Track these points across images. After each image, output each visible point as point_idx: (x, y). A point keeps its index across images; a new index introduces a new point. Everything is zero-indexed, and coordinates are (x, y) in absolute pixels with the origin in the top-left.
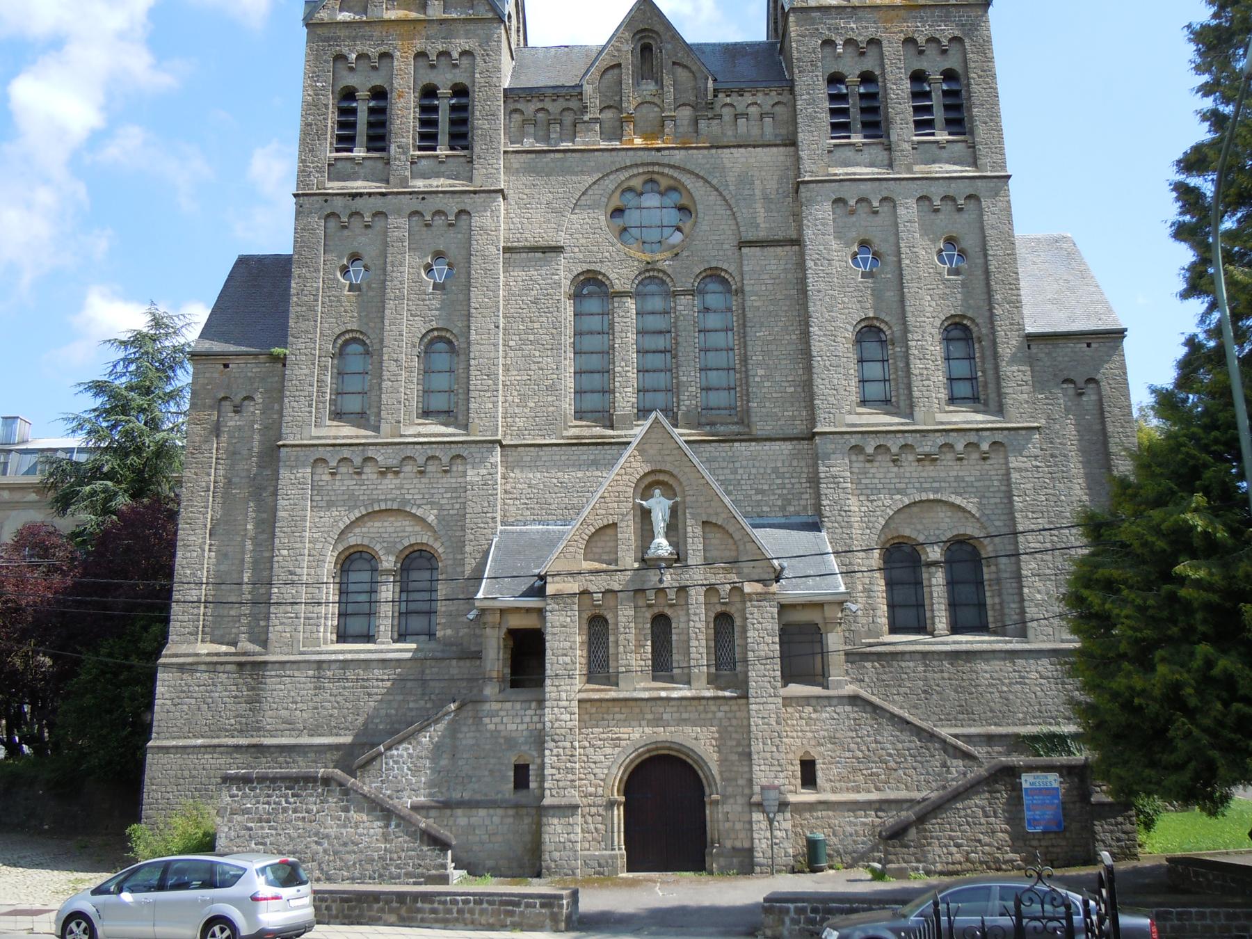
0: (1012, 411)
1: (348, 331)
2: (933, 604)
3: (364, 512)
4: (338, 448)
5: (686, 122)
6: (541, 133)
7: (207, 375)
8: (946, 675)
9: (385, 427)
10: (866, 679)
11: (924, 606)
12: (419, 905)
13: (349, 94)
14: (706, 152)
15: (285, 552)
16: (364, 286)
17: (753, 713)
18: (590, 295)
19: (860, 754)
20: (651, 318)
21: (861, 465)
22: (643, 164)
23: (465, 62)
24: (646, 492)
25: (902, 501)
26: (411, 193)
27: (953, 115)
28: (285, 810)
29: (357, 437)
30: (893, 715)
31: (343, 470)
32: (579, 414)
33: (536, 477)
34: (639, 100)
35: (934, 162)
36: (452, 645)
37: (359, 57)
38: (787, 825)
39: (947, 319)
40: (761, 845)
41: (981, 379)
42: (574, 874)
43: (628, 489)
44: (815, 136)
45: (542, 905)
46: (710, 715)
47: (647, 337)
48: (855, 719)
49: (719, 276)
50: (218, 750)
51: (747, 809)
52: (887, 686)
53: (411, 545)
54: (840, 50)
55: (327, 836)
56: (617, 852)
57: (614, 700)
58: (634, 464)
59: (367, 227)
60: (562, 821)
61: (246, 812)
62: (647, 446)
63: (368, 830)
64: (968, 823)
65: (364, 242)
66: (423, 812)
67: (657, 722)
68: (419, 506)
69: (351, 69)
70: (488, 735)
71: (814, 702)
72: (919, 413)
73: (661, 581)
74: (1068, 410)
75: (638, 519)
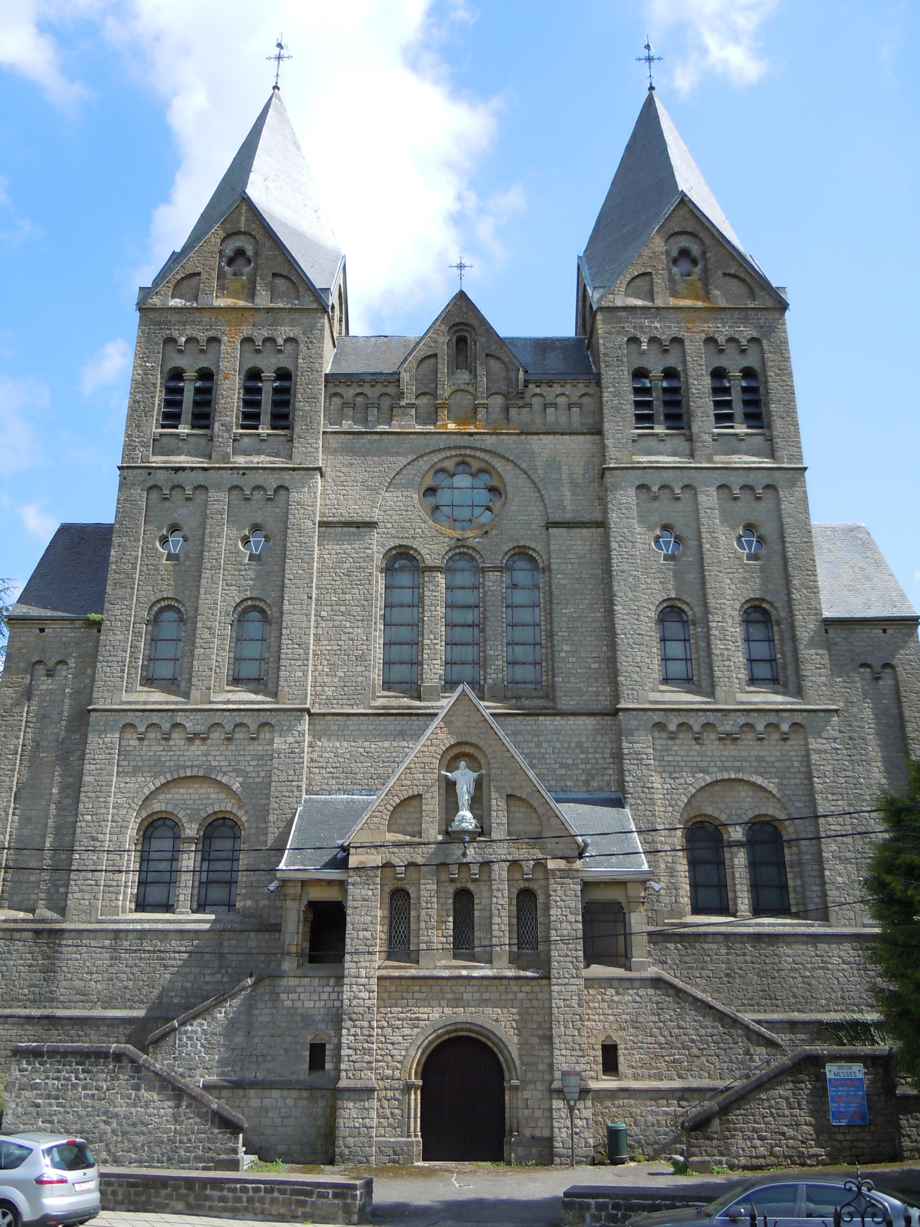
0: (811, 693)
1: (163, 599)
2: (735, 885)
3: (170, 779)
4: (147, 713)
5: (497, 410)
6: (359, 416)
7: (23, 639)
8: (748, 958)
9: (195, 694)
10: (669, 961)
11: (726, 886)
12: (208, 1192)
13: (177, 375)
14: (516, 438)
15: (89, 818)
16: (182, 555)
17: (555, 995)
18: (402, 569)
19: (663, 1040)
20: (460, 592)
21: (664, 742)
22: (455, 448)
23: (289, 348)
24: (451, 762)
25: (704, 780)
26: (232, 469)
27: (751, 410)
28: (74, 1086)
29: (167, 703)
30: (696, 1000)
31: (151, 735)
32: (387, 685)
33: (342, 746)
34: (454, 388)
35: (733, 453)
36: (251, 916)
37: (189, 340)
38: (588, 1113)
39: (747, 602)
40: (561, 1135)
41: (780, 661)
42: (368, 1161)
43: (434, 760)
44: (620, 425)
45: (336, 1196)
46: (511, 996)
47: (456, 611)
48: (657, 1003)
49: (527, 554)
50: (10, 1020)
51: (547, 1096)
52: (690, 968)
53: (215, 813)
54: (644, 347)
55: (116, 1115)
56: (413, 1139)
57: (414, 978)
58: (441, 736)
59: (188, 499)
60: (357, 1105)
61: (35, 1087)
62: (453, 718)
63: (158, 1109)
64: (772, 1114)
65: (183, 513)
66: (215, 1092)
67: (457, 1002)
68: (225, 773)
69: (180, 351)
70: (285, 1012)
71: (616, 984)
72: (720, 692)
73: (464, 855)
74: (865, 695)
75: (443, 791)
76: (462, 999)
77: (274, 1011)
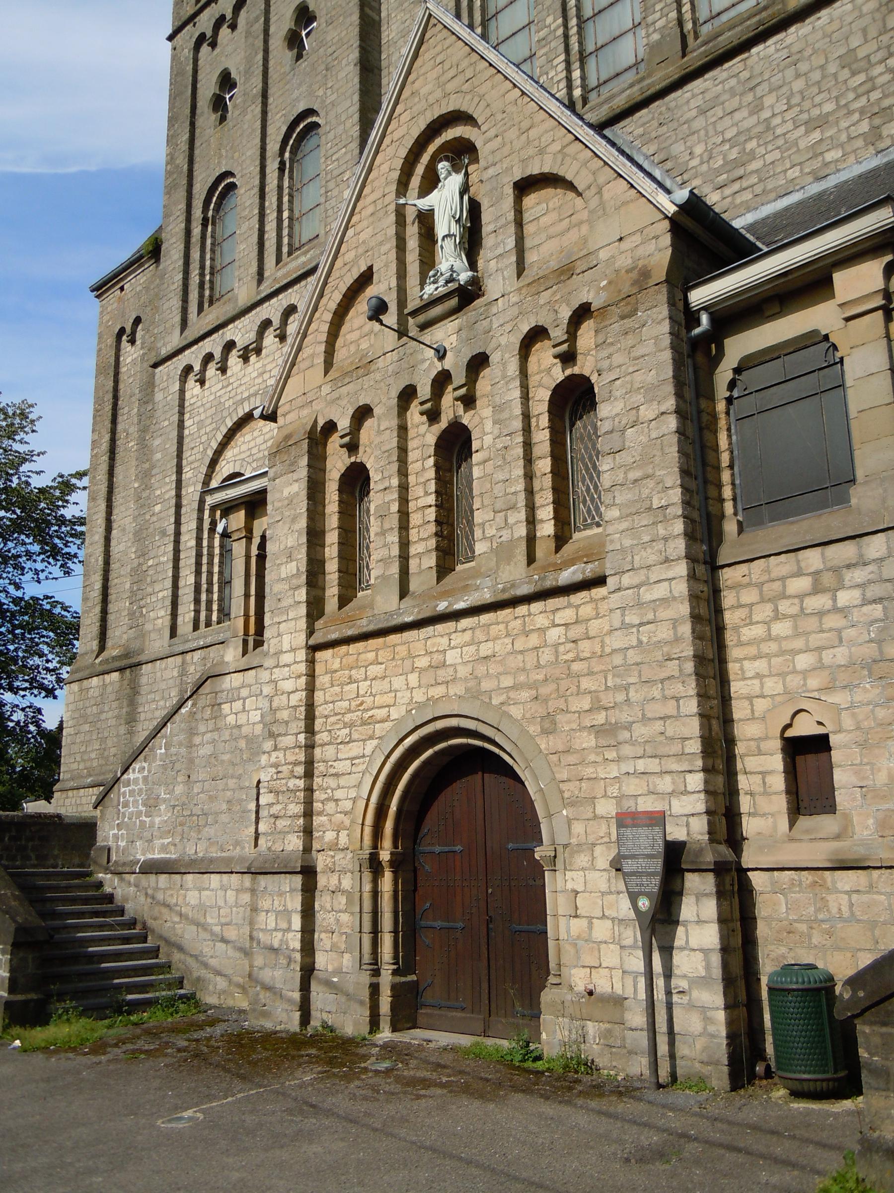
46: (534, 640)
76: (444, 665)
77: (215, 735)
